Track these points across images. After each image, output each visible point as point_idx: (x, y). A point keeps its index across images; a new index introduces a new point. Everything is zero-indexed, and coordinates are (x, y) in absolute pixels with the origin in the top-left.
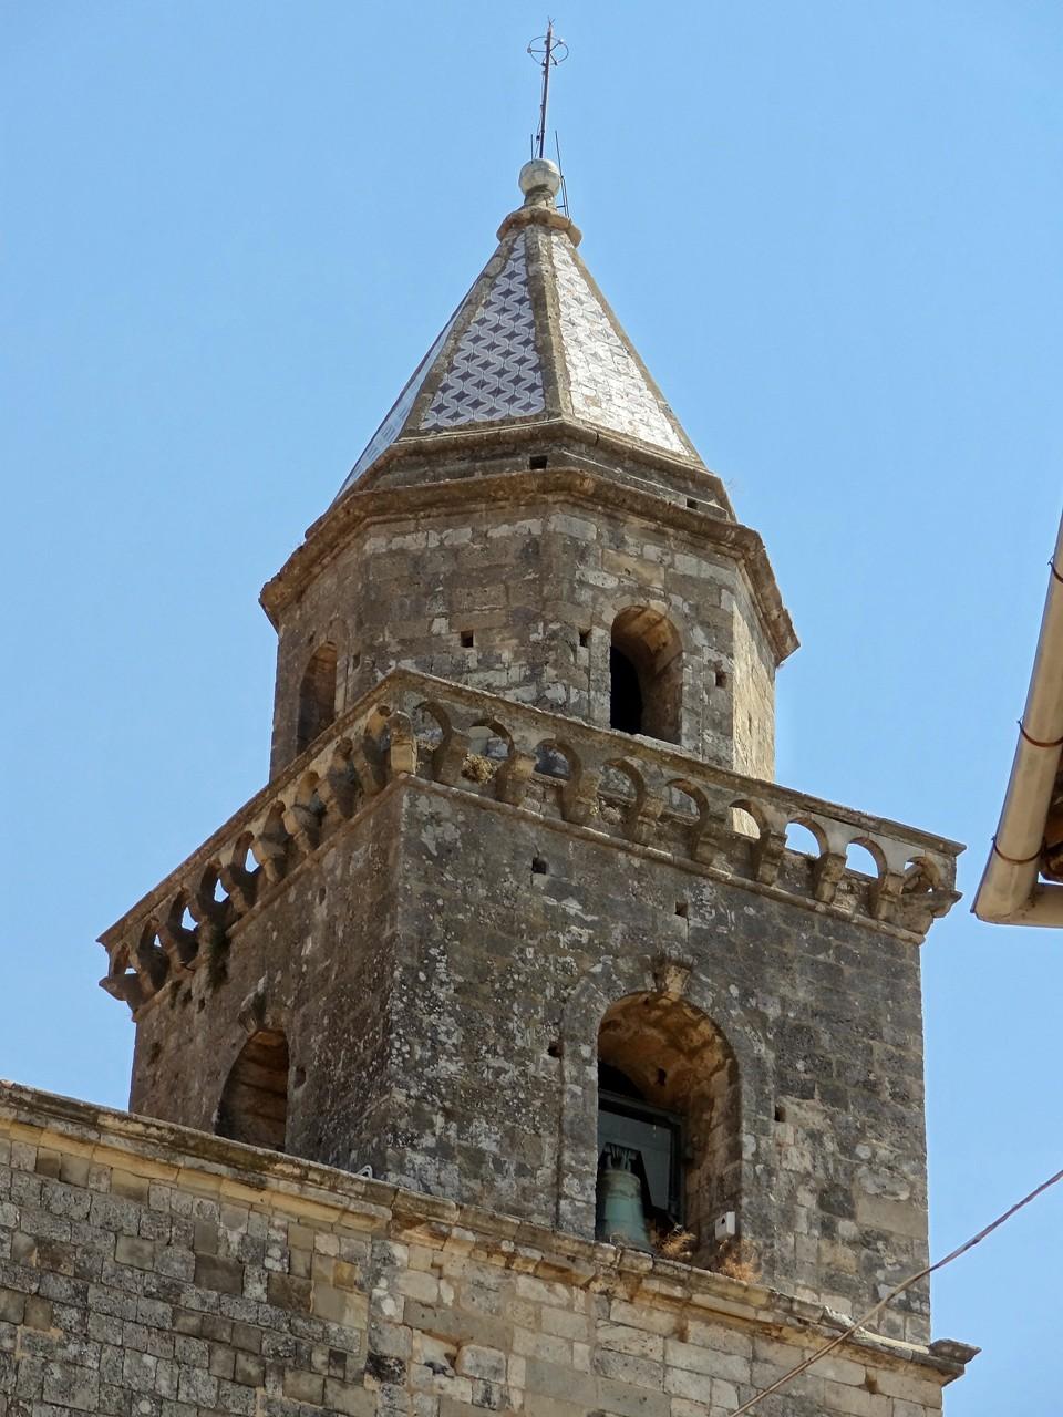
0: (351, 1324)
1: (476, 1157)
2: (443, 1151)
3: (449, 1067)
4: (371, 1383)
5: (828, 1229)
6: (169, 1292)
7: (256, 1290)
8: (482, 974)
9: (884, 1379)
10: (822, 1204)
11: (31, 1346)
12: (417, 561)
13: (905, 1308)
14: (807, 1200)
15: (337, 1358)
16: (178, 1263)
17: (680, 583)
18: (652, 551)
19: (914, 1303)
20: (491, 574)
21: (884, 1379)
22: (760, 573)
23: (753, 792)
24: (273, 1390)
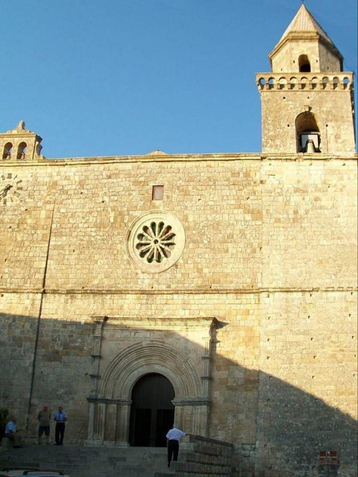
1: (277, 146)
3: (271, 133)
4: (261, 185)
5: (336, 141)
6: (228, 180)
7: (241, 175)
8: (276, 117)
10: (335, 138)
14: (333, 137)
15: (255, 182)
16: (229, 175)
24: (245, 190)
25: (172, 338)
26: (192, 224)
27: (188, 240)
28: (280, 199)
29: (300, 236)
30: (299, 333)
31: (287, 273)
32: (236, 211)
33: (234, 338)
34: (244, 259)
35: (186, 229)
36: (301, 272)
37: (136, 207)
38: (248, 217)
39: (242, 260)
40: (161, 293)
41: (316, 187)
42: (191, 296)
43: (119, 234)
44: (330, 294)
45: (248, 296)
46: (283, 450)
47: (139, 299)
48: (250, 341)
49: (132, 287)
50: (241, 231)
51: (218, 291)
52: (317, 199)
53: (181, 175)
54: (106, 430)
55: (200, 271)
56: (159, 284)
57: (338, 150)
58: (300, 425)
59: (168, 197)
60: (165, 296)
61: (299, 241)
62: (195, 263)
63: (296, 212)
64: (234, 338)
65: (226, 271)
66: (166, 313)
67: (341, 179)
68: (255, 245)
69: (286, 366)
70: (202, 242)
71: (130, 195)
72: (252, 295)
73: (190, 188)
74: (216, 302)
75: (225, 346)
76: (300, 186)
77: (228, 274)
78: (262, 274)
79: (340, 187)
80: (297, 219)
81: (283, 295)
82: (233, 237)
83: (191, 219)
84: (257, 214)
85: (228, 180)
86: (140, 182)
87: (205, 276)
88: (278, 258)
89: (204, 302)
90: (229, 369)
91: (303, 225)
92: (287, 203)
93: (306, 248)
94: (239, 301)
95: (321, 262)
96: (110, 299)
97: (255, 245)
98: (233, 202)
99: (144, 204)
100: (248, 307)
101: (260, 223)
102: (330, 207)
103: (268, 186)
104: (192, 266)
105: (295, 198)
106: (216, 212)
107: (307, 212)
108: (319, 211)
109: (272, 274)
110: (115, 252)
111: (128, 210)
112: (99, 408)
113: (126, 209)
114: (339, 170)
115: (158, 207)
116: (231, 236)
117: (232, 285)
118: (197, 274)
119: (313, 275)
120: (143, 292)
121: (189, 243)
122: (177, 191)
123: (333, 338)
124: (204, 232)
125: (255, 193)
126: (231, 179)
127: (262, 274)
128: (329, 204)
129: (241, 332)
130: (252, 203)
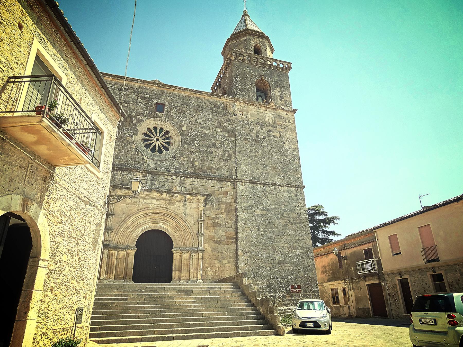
0: (231, 111)
2: (240, 94)
5: (281, 100)
6: (212, 109)
8: (243, 78)
9: (288, 113)
11: (197, 114)
12: (234, 44)
13: (289, 107)
15: (230, 114)
16: (212, 106)
17: (261, 42)
18: (257, 39)
19: (291, 106)
20: (241, 43)
21: (288, 113)
22: (269, 41)
23: (269, 59)
25: (174, 205)
26: (186, 132)
27: (184, 141)
28: (247, 127)
29: (260, 151)
30: (263, 209)
31: (253, 172)
32: (217, 129)
33: (218, 209)
34: (224, 160)
35: (182, 135)
36: (262, 172)
37: (143, 114)
38: (226, 134)
39: (222, 160)
40: (163, 174)
41: (269, 123)
42: (186, 179)
43: (128, 130)
44: (281, 188)
45: (226, 183)
46: (257, 284)
47: (144, 176)
48: (229, 211)
49: (139, 167)
50: (221, 142)
51: (207, 178)
52: (270, 131)
53: (178, 100)
54: (116, 271)
55: (192, 163)
56: (161, 168)
57: (282, 105)
58: (268, 268)
59: (168, 112)
60: (166, 177)
61: (259, 153)
62: (189, 158)
63: (257, 136)
64: (218, 209)
65: (211, 165)
66: (167, 188)
67: (285, 122)
68: (231, 152)
69: (256, 229)
70: (194, 145)
71: (138, 105)
72: (229, 183)
73: (184, 109)
74: (204, 184)
75: (212, 214)
76: (260, 121)
77: (212, 167)
78: (236, 170)
79: (284, 126)
80: (258, 140)
81: (251, 185)
82: (215, 145)
83: (184, 128)
84: (232, 134)
85: (212, 109)
86: (146, 98)
87: (196, 167)
88: (247, 162)
89: (195, 183)
90: (215, 229)
91: (262, 144)
92: (251, 130)
93: (265, 159)
94: (221, 186)
95: (274, 168)
96: (121, 174)
97: (231, 152)
98: (215, 123)
99: (149, 113)
100: (227, 190)
101: (234, 139)
102: (278, 137)
103: (239, 118)
104: (187, 159)
105: (256, 128)
106: (204, 128)
107: (264, 137)
108: (272, 138)
109: (243, 171)
110: (125, 142)
111: (135, 115)
112: (111, 254)
113: (134, 114)
114: (283, 117)
115: (160, 117)
116: (214, 144)
117: (216, 175)
118: (190, 165)
119: (269, 175)
120: (148, 172)
121: (184, 144)
122: (175, 109)
123: (285, 214)
124: (195, 139)
125: (230, 121)
126: (214, 109)
127: (236, 170)
128: (278, 135)
129: (222, 206)
130: (228, 126)
